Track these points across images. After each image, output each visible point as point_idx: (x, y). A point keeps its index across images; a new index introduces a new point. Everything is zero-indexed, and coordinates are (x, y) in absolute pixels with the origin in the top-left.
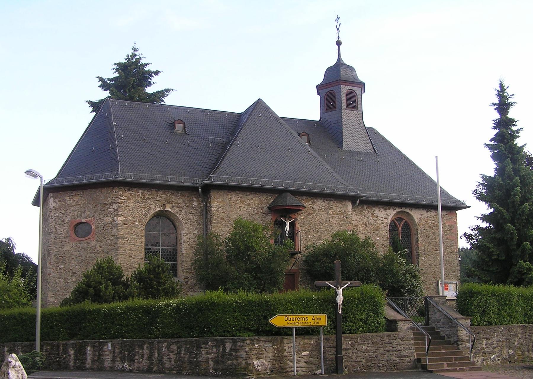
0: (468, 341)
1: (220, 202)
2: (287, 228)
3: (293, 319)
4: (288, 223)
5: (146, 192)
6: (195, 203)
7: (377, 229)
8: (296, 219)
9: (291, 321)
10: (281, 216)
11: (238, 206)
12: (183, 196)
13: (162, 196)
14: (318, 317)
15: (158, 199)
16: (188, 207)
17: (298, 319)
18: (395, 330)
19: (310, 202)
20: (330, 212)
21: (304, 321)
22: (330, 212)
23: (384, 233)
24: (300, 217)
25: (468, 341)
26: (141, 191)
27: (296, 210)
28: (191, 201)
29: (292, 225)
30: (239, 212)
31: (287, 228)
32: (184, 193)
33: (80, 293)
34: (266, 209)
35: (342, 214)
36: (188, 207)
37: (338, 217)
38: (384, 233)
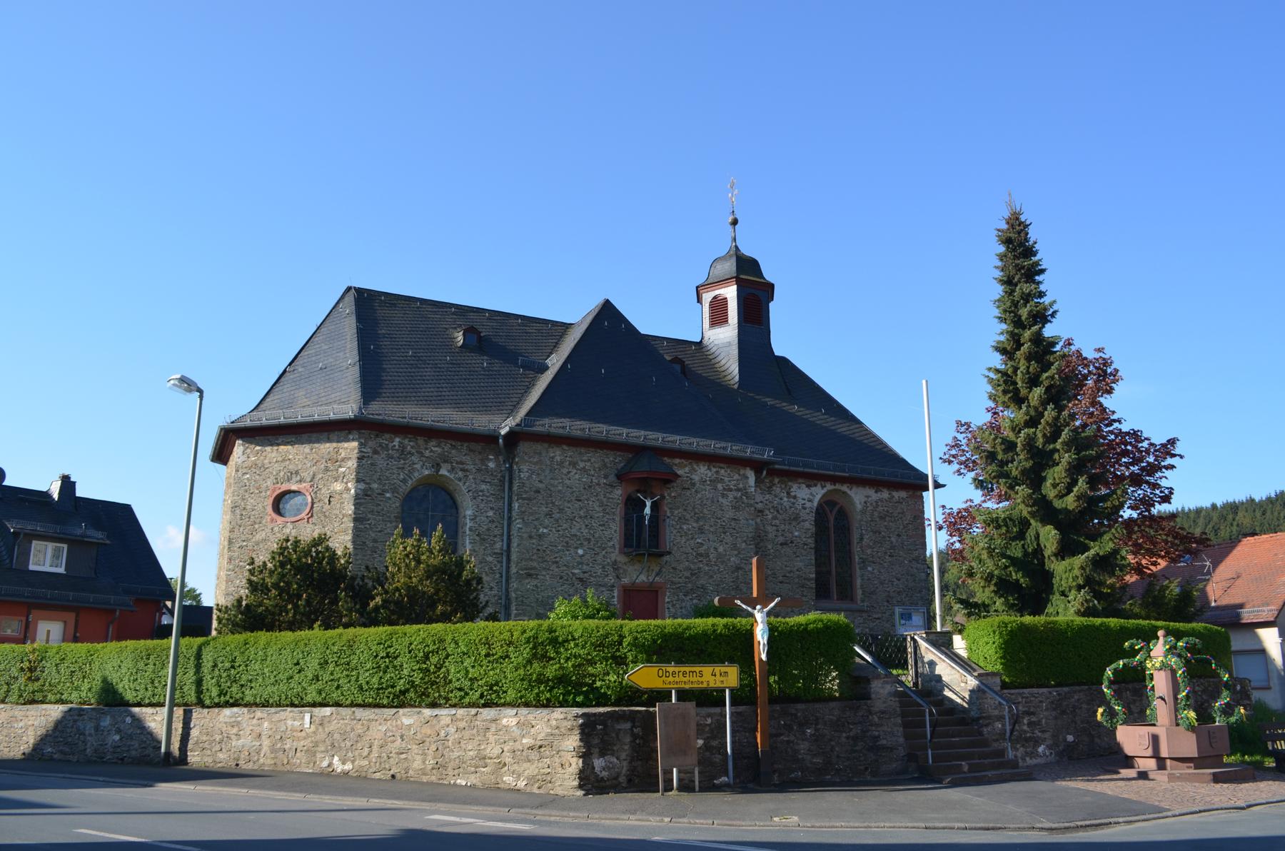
0: (1001, 718)
1: (535, 464)
2: (647, 510)
3: (674, 673)
4: (648, 504)
5: (406, 442)
6: (492, 465)
7: (796, 518)
8: (663, 497)
9: (671, 679)
10: (638, 491)
11: (565, 471)
12: (471, 450)
13: (434, 448)
14: (723, 669)
15: (427, 453)
16: (479, 470)
17: (684, 673)
18: (867, 697)
19: (687, 469)
20: (720, 486)
21: (695, 679)
22: (720, 486)
23: (807, 525)
24: (670, 494)
25: (1001, 718)
26: (397, 440)
27: (669, 479)
28: (484, 461)
29: (655, 506)
30: (567, 482)
31: (647, 510)
32: (473, 445)
33: (1074, 467)
34: (612, 478)
35: (738, 490)
36: (479, 470)
37: (731, 495)
38: (807, 525)
